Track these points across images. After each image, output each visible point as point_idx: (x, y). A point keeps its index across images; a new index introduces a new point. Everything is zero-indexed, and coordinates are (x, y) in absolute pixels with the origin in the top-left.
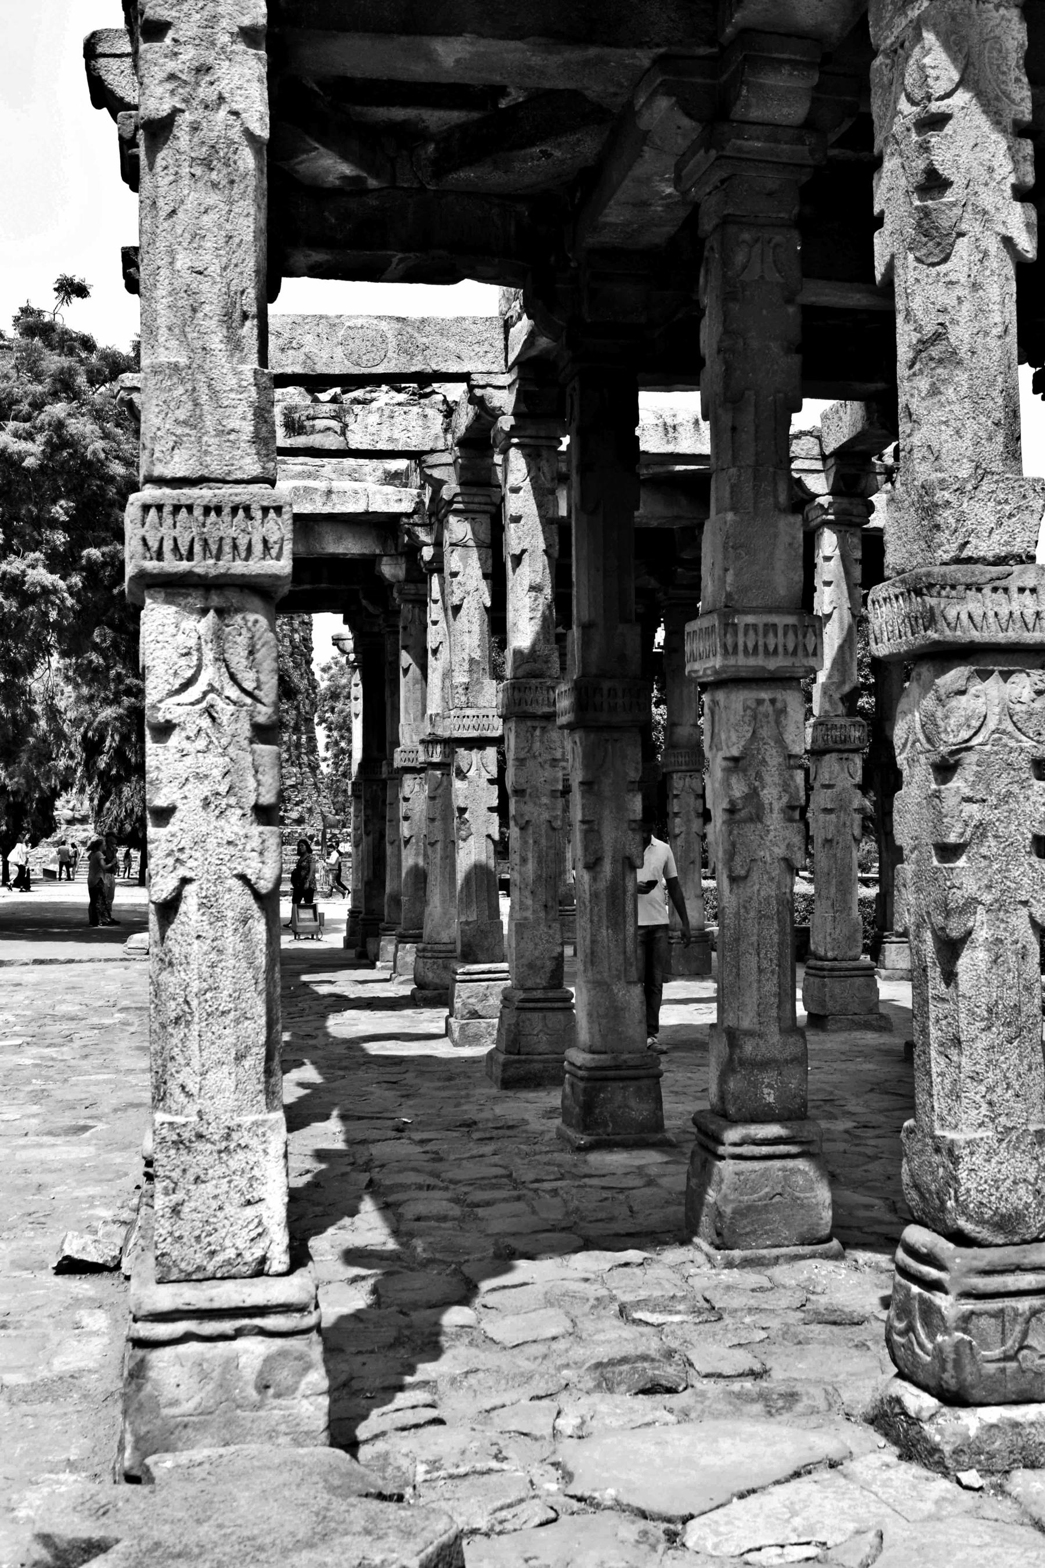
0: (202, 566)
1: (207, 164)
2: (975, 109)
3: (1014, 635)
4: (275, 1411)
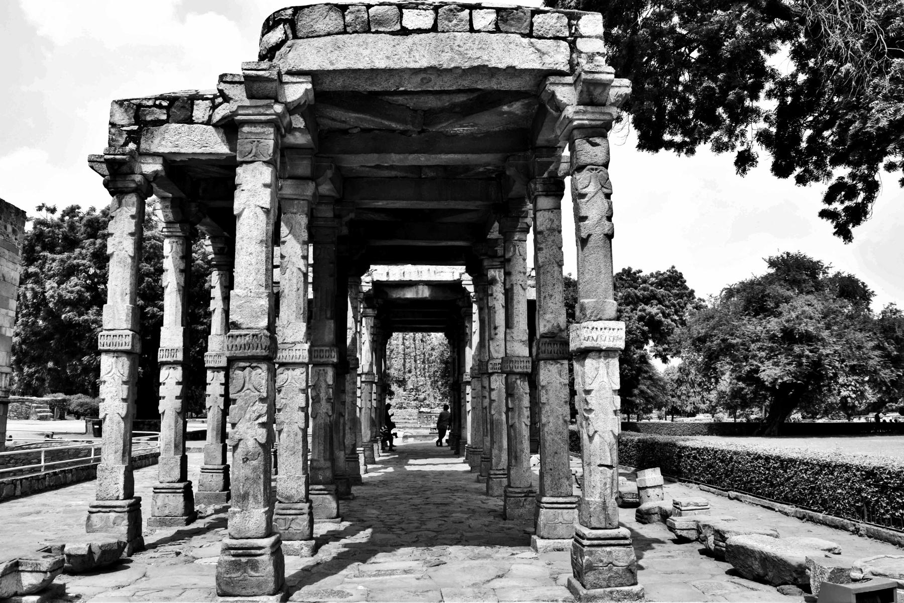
0: (111, 348)
1: (120, 262)
2: (293, 239)
3: (294, 360)
4: (116, 528)
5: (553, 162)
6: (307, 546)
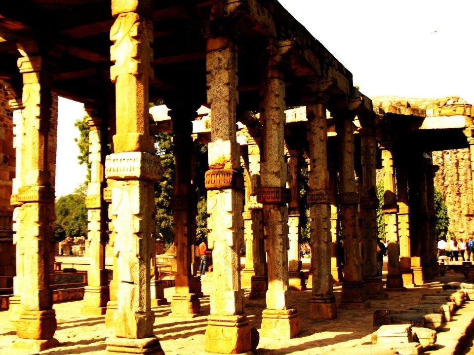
5: (212, 5)
6: (37, 343)
